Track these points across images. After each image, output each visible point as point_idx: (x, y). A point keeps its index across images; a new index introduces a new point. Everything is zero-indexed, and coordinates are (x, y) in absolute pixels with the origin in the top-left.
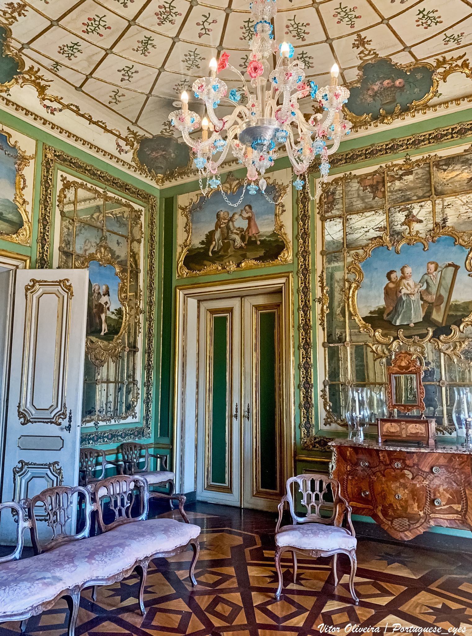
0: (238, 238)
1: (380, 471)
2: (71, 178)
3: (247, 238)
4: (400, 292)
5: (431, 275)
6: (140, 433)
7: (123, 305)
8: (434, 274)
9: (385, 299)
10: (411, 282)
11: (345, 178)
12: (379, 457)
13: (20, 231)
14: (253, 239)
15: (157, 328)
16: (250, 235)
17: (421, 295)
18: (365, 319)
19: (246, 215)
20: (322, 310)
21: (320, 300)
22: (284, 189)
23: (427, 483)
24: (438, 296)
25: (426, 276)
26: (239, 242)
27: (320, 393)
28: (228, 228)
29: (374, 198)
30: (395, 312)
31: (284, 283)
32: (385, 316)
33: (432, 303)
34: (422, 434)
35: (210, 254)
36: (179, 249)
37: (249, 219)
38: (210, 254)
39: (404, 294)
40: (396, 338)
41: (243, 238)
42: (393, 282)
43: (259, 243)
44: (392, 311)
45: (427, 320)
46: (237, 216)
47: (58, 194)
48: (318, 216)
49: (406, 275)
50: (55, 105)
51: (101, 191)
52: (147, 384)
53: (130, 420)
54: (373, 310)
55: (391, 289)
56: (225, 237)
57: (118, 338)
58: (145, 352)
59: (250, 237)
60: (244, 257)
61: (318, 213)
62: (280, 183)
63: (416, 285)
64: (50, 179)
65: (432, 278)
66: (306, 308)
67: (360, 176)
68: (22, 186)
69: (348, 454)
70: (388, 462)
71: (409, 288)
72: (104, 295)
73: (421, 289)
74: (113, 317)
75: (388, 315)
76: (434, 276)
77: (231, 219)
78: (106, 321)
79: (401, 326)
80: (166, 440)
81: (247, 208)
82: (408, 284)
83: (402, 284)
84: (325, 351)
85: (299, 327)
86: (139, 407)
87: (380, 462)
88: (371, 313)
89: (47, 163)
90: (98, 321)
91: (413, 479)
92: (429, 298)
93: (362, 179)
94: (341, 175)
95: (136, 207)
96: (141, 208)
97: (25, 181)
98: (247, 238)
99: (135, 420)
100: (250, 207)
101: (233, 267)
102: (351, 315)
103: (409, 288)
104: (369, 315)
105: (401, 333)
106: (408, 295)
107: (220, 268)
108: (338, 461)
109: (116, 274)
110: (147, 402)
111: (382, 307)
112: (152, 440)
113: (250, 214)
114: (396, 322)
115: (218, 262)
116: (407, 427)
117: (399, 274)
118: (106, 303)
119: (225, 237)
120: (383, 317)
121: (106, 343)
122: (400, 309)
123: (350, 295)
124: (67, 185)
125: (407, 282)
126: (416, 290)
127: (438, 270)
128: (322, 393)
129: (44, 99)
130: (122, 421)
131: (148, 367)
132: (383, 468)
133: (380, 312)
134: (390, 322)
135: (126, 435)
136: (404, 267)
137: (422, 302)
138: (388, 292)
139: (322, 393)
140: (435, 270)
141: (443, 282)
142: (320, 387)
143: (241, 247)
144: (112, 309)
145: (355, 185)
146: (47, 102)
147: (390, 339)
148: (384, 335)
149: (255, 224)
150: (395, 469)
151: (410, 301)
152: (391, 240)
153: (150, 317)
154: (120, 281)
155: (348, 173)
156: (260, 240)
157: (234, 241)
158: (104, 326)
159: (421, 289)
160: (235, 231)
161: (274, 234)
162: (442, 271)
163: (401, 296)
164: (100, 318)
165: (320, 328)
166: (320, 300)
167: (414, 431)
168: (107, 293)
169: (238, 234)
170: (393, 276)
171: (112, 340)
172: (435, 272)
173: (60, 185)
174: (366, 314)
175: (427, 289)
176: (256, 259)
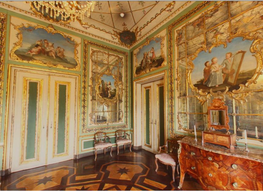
0: (149, 60)
1: (201, 160)
2: (95, 49)
3: (152, 60)
4: (211, 71)
5: (228, 60)
6: (124, 127)
7: (116, 87)
8: (230, 59)
9: (204, 75)
10: (217, 65)
11: (186, 26)
12: (200, 152)
13: (76, 67)
14: (154, 60)
15: (129, 94)
16: (153, 58)
17: (222, 71)
18: (195, 85)
19: (152, 52)
20: (177, 83)
21: (177, 79)
22: (163, 38)
23: (228, 172)
24: (232, 69)
25: (225, 61)
26: (150, 62)
27: (176, 117)
28: (147, 57)
29: (199, 30)
30: (208, 80)
31: (164, 74)
32: (204, 83)
33: (228, 74)
34: (226, 142)
35: (142, 68)
36: (134, 68)
37: (153, 53)
38: (142, 68)
39: (213, 72)
40: (209, 93)
41: (151, 60)
42: (208, 67)
43: (156, 61)
44: (207, 81)
45: (226, 83)
46: (149, 53)
47: (90, 54)
48: (176, 45)
49: (214, 62)
50: (86, 26)
51: (107, 52)
52: (126, 112)
53: (120, 123)
54: (198, 81)
55: (207, 70)
56: (146, 61)
57: (115, 98)
58: (125, 102)
59: (153, 59)
60: (151, 67)
61: (176, 44)
62: (162, 36)
63: (219, 66)
64: (87, 50)
65: (229, 61)
66: (171, 83)
67: (192, 22)
68: (76, 53)
69: (186, 147)
70: (205, 156)
71: (216, 68)
72: (109, 85)
73: (222, 67)
74: (113, 91)
75: (205, 82)
76: (229, 60)
77: (148, 54)
78: (110, 93)
79: (211, 87)
80: (132, 129)
81: (152, 49)
82: (215, 67)
83: (212, 67)
84: (179, 100)
85: (169, 91)
86: (124, 119)
87: (201, 155)
88: (197, 82)
89: (85, 45)
90: (107, 93)
91: (219, 168)
92: (226, 72)
93: (193, 24)
94: (185, 25)
95: (120, 56)
96: (122, 57)
97: (77, 51)
98: (152, 60)
99: (122, 123)
100: (153, 48)
101: (148, 71)
102: (189, 84)
103: (216, 68)
104: (197, 83)
105: (211, 90)
106: (215, 72)
107: (145, 72)
108: (182, 149)
109: (113, 78)
110: (126, 117)
111: (202, 79)
112: (129, 129)
113: (153, 51)
114: (209, 85)
115: (144, 70)
116: (217, 138)
117: (210, 63)
118: (110, 87)
119: (146, 61)
120: (203, 83)
121: (110, 100)
122: (211, 79)
123: (188, 76)
124: (94, 52)
125: (215, 65)
126: (220, 68)
127: (232, 57)
128: (177, 117)
129: (82, 24)
130: (117, 123)
131: (126, 107)
132: (202, 158)
133: (202, 81)
134: (206, 86)
135: (119, 127)
136: (213, 59)
137: (223, 74)
138: (205, 72)
139: (177, 117)
140: (231, 57)
141: (235, 62)
142: (177, 114)
143: (151, 64)
144: (112, 89)
145: (191, 28)
146: (83, 25)
147: (206, 94)
148: (203, 92)
149: (155, 54)
150: (208, 160)
151: (216, 75)
152: (206, 47)
153: (127, 91)
154: (115, 80)
155: (187, 23)
156: (156, 60)
157: (148, 62)
158: (109, 95)
159: (222, 67)
160: (149, 58)
161: (161, 56)
162: (234, 57)
163: (211, 73)
164: (108, 92)
165: (177, 91)
166: (177, 79)
167: (222, 140)
168: (110, 84)
169: (149, 59)
170: (208, 64)
171: (113, 98)
172: (230, 58)
173: (91, 52)
174: (195, 83)
175: (226, 66)
176: (155, 67)
